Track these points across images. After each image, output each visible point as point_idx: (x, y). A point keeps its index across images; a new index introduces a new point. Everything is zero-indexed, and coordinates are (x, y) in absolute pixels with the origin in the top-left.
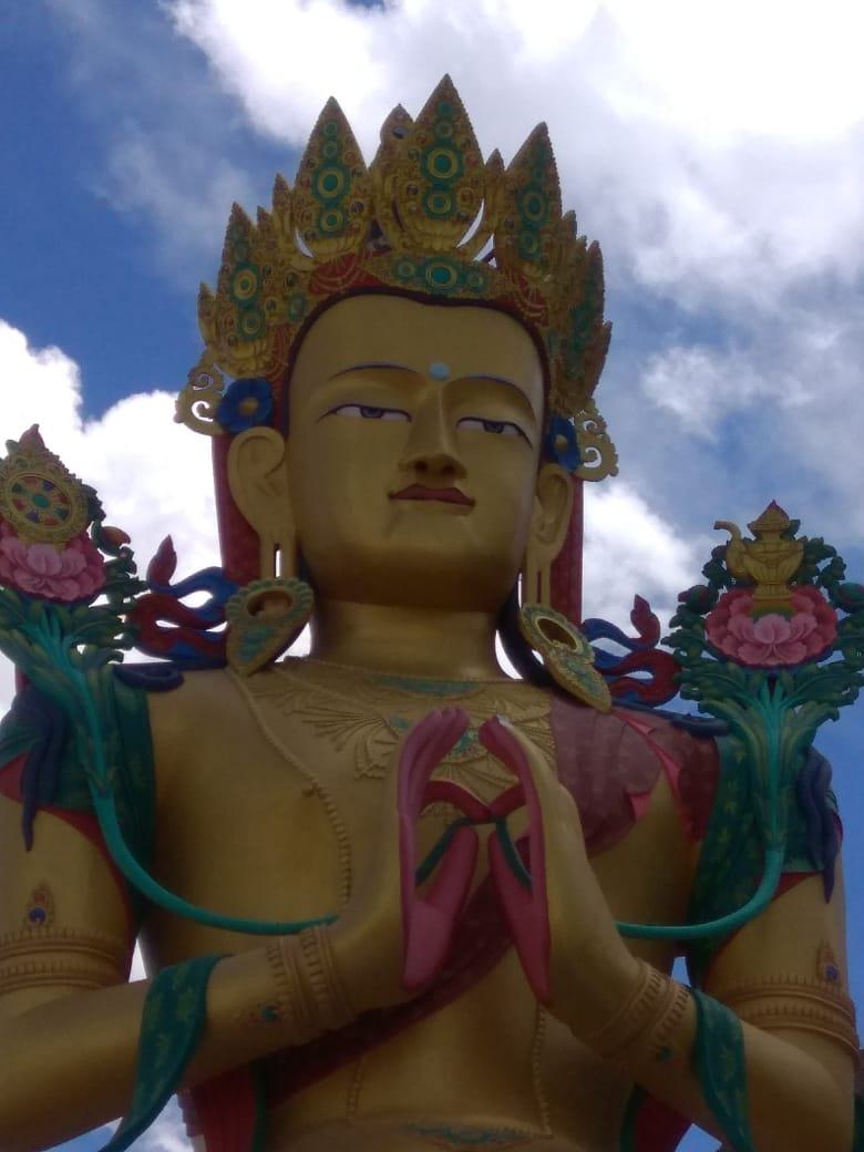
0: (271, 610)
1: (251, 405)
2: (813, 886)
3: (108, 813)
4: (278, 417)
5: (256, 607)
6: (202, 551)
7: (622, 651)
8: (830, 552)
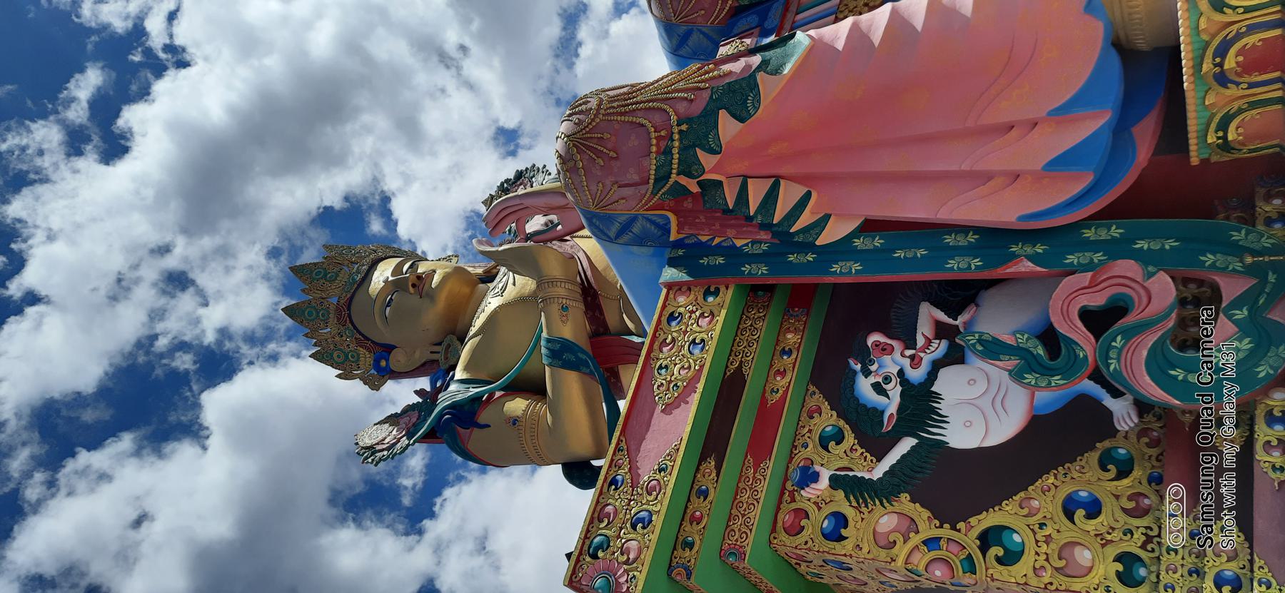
1: (383, 363)
4: (389, 349)
8: (502, 184)
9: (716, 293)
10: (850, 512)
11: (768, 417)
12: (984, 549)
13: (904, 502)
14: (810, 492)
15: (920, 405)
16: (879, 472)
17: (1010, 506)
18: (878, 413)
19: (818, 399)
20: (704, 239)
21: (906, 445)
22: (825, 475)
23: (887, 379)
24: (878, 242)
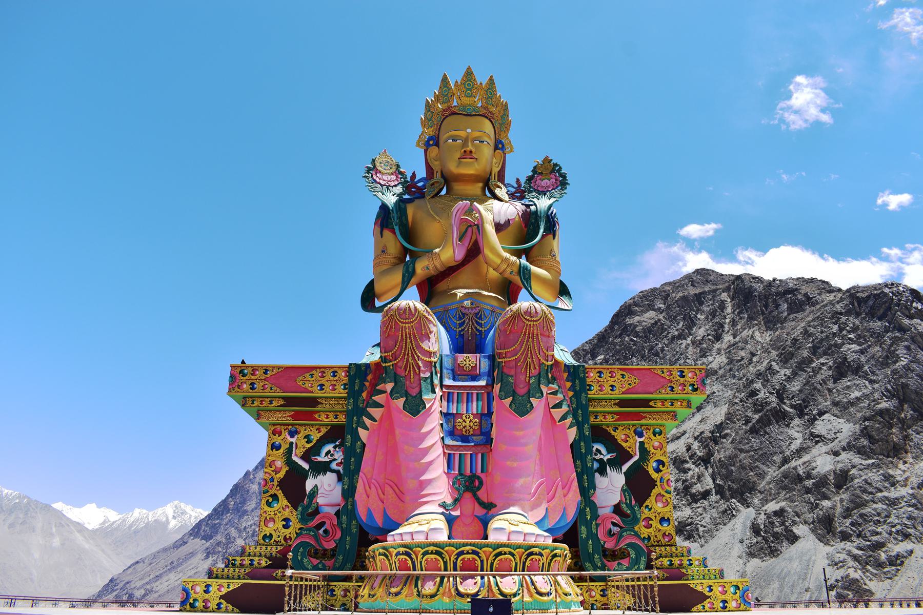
0: (436, 185)
2: (551, 236)
3: (397, 229)
4: (437, 144)
5: (433, 184)
6: (421, 173)
7: (514, 190)
9: (345, 389)
10: (281, 451)
11: (310, 416)
12: (271, 496)
15: (323, 468)
16: (294, 458)
17: (286, 502)
19: (324, 430)
20: (369, 378)
21: (306, 466)
22: (293, 440)
23: (332, 455)
24: (358, 451)
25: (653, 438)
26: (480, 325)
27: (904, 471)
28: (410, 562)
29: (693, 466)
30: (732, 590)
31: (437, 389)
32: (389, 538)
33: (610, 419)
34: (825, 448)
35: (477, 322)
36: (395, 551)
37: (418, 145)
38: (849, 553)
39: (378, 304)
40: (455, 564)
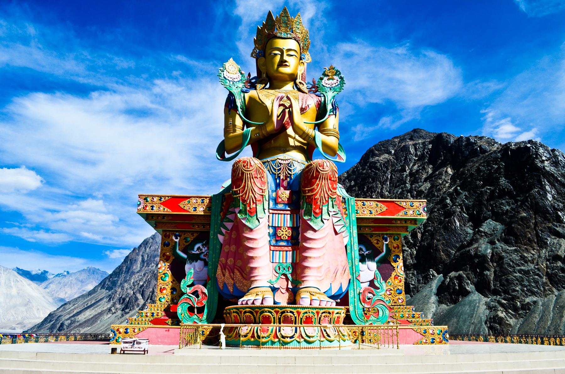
6: (254, 74)
7: (310, 86)
10: (170, 246)
12: (164, 274)
13: (172, 258)
14: (174, 238)
18: (193, 249)
19: (195, 235)
20: (224, 204)
21: (185, 256)
22: (177, 240)
23: (201, 250)
25: (393, 242)
26: (290, 170)
27: (533, 254)
28: (252, 317)
29: (407, 249)
30: (438, 332)
31: (266, 211)
32: (239, 303)
33: (367, 231)
34: (487, 240)
35: (289, 169)
36: (244, 311)
37: (252, 56)
38: (499, 302)
39: (227, 156)
40: (280, 319)
